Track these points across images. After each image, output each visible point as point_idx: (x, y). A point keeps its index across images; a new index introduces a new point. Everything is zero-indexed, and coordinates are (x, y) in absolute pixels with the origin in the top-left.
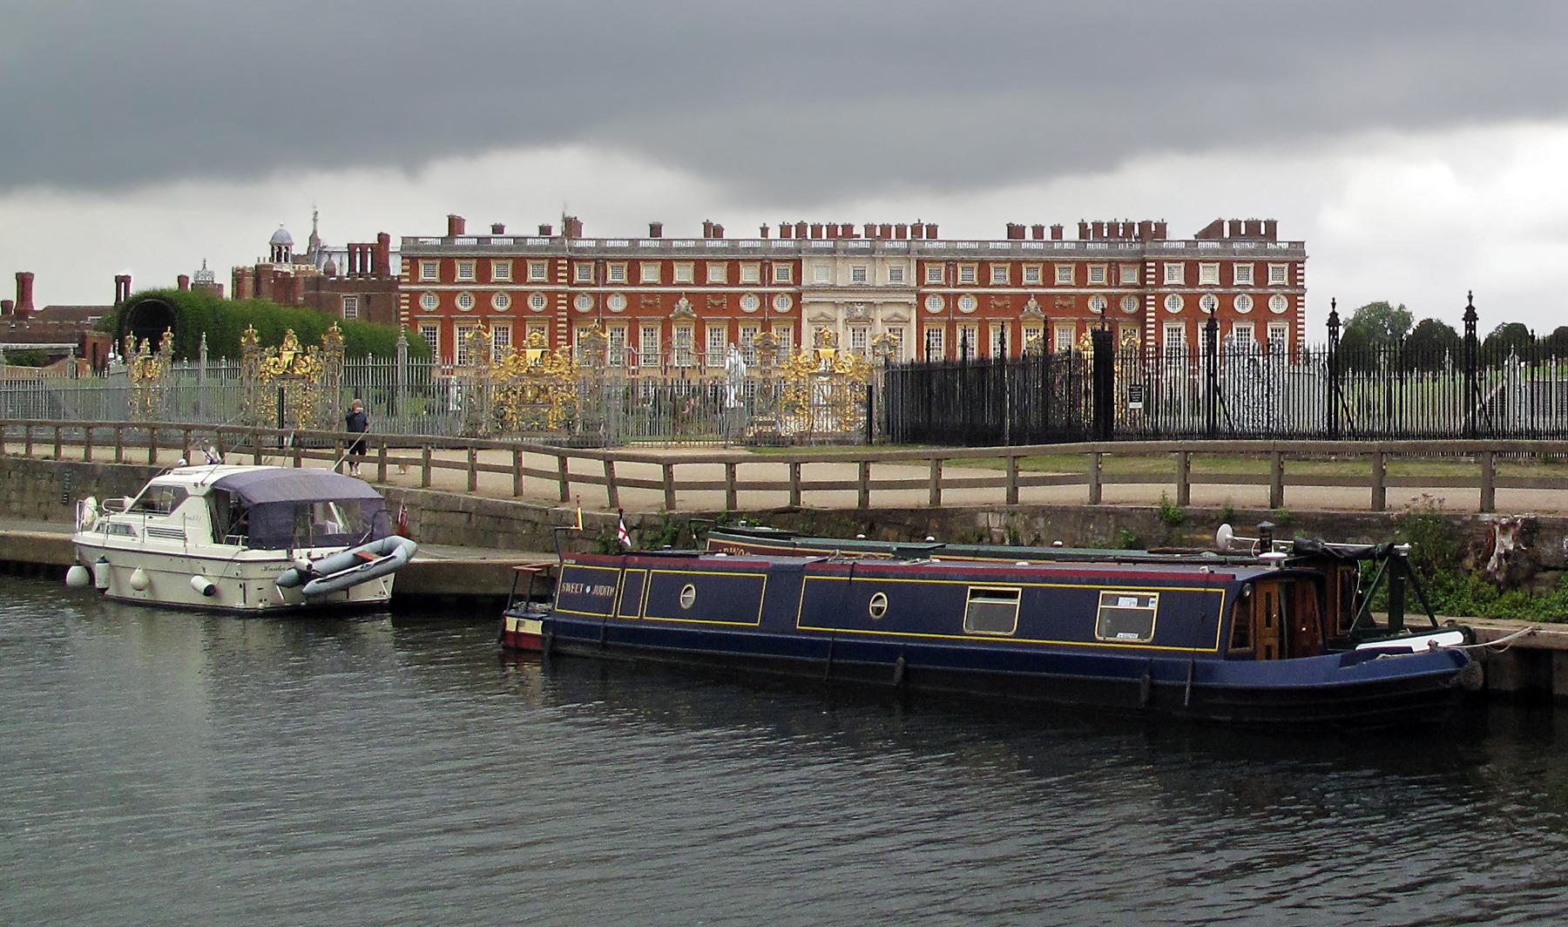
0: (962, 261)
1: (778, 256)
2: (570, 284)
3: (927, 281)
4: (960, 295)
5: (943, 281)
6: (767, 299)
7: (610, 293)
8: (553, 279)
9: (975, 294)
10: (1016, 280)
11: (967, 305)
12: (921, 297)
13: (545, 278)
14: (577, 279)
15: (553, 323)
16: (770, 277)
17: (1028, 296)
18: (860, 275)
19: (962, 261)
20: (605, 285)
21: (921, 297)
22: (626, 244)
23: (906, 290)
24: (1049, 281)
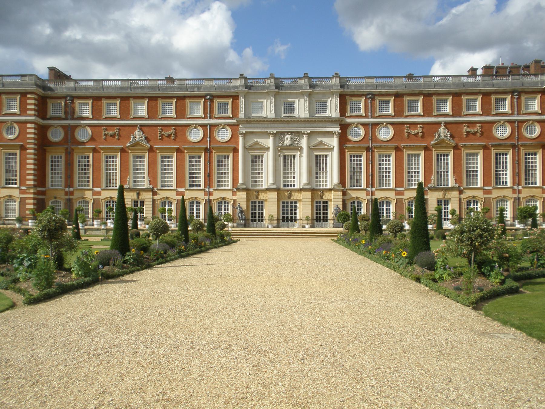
0: (381, 95)
1: (218, 93)
2: (44, 118)
3: (348, 114)
4: (378, 124)
5: (362, 112)
6: (209, 130)
7: (76, 126)
8: (23, 110)
9: (392, 124)
10: (427, 111)
11: (386, 134)
12: (344, 127)
13: (16, 111)
14: (50, 113)
15: (23, 148)
16: (212, 112)
17: (439, 123)
18: (290, 107)
19: (381, 95)
20: (73, 118)
21: (344, 127)
22: (91, 83)
23: (330, 121)
24: (457, 111)
